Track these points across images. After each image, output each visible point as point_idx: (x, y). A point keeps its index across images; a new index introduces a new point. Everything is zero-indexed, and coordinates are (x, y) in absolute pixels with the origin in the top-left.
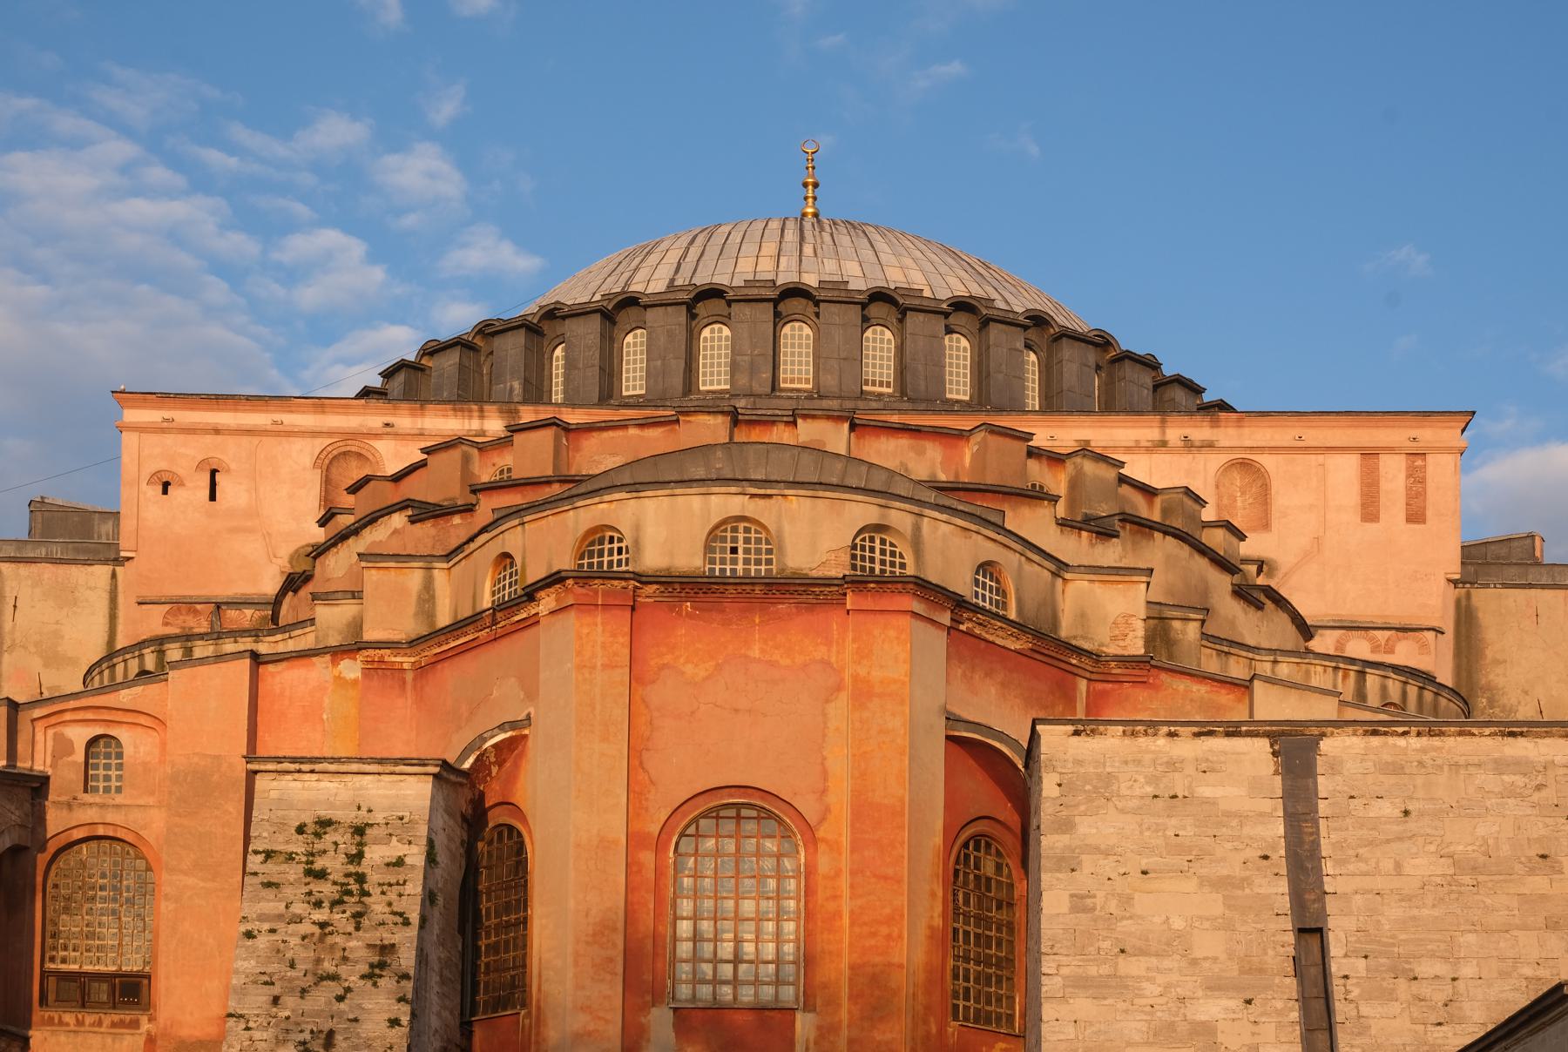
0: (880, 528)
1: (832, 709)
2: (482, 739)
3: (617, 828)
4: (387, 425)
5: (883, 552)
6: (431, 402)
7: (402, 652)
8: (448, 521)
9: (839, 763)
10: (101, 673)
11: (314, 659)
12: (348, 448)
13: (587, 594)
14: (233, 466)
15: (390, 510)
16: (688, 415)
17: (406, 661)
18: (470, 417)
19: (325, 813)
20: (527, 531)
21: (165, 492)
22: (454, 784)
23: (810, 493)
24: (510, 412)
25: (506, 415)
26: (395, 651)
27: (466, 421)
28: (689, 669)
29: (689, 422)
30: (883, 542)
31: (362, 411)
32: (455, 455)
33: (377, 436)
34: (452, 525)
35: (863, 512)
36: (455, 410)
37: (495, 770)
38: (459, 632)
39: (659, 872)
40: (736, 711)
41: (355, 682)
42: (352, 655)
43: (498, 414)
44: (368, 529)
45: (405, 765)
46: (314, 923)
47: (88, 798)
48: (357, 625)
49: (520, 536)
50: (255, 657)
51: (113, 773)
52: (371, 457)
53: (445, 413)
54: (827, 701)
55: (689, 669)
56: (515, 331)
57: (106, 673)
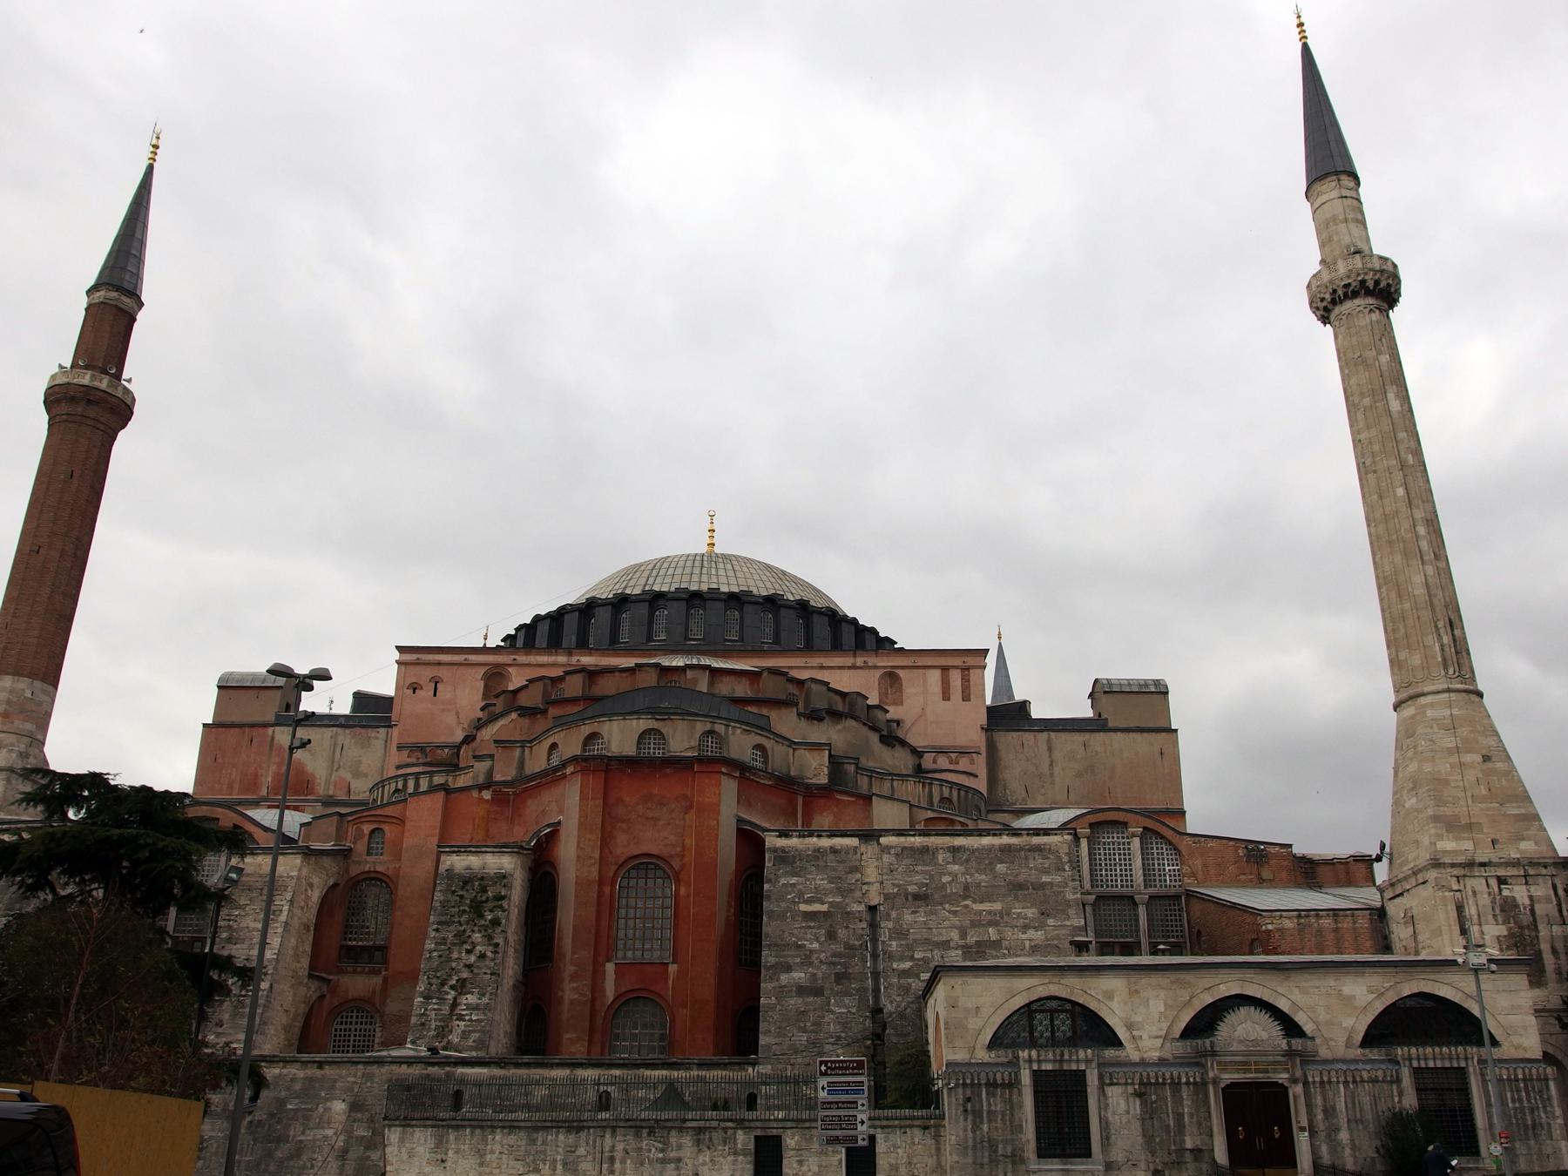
0: (711, 732)
1: (687, 816)
2: (540, 831)
3: (595, 874)
4: (515, 659)
5: (712, 742)
9: (690, 842)
10: (378, 789)
14: (445, 680)
18: (551, 655)
21: (414, 693)
22: (526, 854)
23: (681, 718)
28: (628, 799)
30: (712, 738)
32: (541, 684)
33: (510, 665)
35: (701, 727)
37: (544, 845)
39: (612, 896)
40: (647, 818)
41: (488, 801)
47: (368, 858)
48: (490, 773)
50: (446, 789)
51: (380, 846)
54: (686, 813)
55: (628, 799)
57: (380, 789)
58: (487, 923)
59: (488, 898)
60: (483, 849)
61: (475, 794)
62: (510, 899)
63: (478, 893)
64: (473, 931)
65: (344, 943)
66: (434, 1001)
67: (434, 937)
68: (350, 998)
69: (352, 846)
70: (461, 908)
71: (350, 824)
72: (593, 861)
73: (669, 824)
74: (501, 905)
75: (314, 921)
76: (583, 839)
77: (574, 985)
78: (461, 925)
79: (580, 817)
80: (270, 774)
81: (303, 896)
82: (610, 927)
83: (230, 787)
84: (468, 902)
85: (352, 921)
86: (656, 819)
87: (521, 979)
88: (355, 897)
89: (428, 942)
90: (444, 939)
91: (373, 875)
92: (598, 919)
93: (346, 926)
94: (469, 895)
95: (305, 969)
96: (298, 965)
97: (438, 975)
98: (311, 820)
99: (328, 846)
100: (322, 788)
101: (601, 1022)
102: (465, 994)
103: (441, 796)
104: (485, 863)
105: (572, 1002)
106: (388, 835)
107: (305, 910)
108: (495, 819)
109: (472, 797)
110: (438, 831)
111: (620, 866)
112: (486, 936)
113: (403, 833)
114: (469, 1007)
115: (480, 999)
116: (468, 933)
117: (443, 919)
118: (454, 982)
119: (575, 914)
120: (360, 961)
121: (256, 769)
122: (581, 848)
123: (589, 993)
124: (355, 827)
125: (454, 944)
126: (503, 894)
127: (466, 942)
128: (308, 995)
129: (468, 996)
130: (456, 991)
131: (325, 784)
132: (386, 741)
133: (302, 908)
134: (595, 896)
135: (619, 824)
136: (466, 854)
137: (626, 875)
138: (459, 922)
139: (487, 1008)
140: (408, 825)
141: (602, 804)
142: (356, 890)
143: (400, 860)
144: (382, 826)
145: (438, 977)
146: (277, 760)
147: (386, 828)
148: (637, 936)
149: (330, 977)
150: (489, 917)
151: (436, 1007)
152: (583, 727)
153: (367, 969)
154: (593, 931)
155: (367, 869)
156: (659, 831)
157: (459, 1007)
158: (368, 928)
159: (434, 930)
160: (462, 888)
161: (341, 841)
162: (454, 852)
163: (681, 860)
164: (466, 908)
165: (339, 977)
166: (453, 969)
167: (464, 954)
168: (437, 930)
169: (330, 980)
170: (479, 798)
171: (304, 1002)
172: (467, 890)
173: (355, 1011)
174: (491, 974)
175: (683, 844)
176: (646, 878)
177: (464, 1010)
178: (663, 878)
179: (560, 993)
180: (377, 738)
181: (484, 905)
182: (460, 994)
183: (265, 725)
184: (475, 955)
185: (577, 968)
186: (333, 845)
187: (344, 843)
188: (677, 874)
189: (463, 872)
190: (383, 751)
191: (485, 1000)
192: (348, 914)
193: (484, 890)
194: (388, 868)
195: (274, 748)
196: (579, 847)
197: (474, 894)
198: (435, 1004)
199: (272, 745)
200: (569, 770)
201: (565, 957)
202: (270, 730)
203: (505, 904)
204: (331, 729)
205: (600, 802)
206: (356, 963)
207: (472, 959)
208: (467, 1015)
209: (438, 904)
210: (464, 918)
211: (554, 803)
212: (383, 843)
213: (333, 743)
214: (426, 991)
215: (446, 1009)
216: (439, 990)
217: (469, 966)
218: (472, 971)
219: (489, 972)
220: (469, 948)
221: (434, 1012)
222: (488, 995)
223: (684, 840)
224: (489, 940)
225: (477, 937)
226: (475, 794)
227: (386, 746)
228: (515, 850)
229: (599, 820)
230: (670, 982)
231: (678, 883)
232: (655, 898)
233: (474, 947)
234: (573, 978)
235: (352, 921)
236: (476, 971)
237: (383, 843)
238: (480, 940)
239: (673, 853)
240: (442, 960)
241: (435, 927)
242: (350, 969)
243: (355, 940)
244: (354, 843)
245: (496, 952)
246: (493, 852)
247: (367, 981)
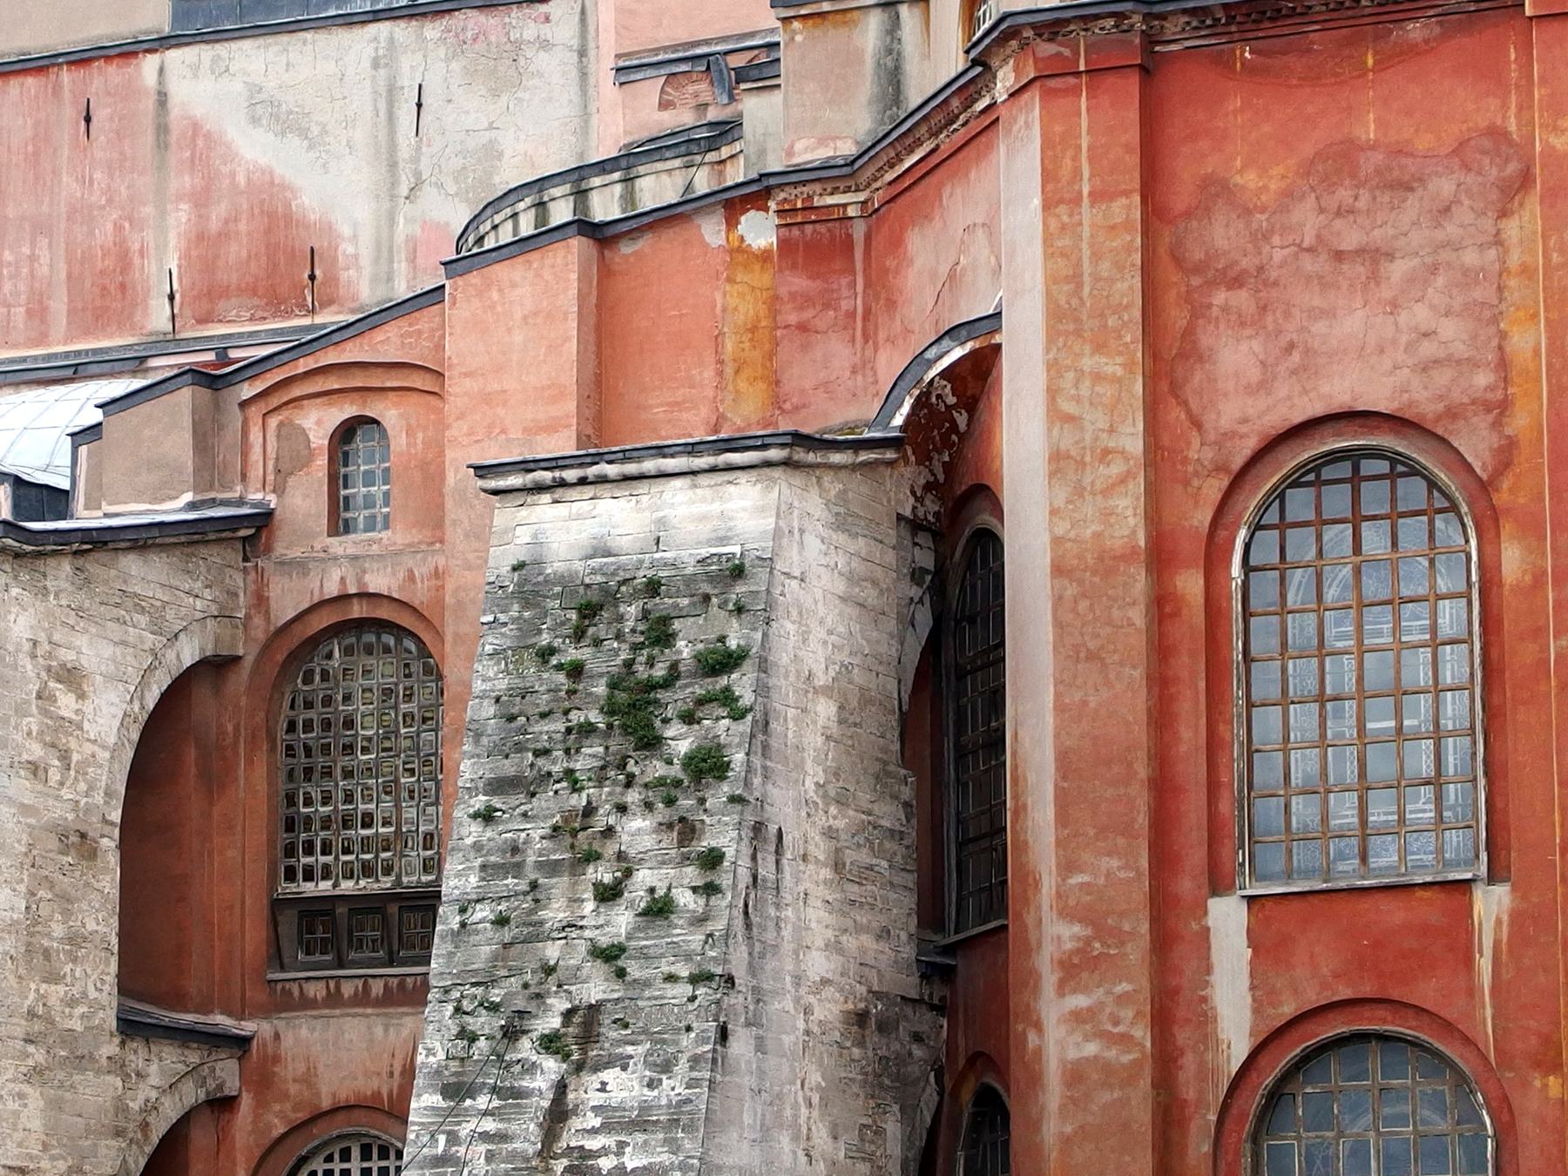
1: (1511, 229)
9: (1528, 341)
22: (854, 467)
37: (962, 419)
40: (1339, 256)
41: (764, 256)
47: (339, 545)
54: (1503, 214)
58: (676, 771)
59: (674, 666)
60: (649, 466)
61: (712, 230)
62: (764, 666)
63: (636, 648)
64: (622, 809)
65: (287, 889)
66: (482, 1101)
67: (477, 847)
68: (326, 1104)
69: (273, 501)
70: (576, 717)
71: (255, 412)
72: (1116, 468)
73: (1434, 269)
74: (727, 689)
75: (116, 816)
76: (1070, 375)
77: (1079, 1001)
78: (576, 787)
79: (1052, 280)
80: (173, 241)
81: (33, 723)
82: (1214, 745)
83: (38, 312)
84: (601, 689)
85: (308, 802)
86: (1375, 256)
87: (910, 985)
88: (309, 705)
89: (451, 866)
90: (515, 849)
91: (357, 611)
92: (1161, 719)
93: (290, 826)
94: (603, 662)
95: (96, 1006)
96: (56, 992)
97: (496, 995)
98: (97, 416)
99: (174, 509)
100: (367, 272)
101: (1206, 1148)
102: (596, 1069)
103: (572, 253)
104: (662, 523)
105: (1075, 1075)
106: (399, 441)
107: (54, 776)
108: (803, 328)
109: (706, 245)
110: (571, 406)
111: (1239, 480)
112: (670, 826)
113: (442, 425)
114: (618, 1122)
115: (651, 1085)
116: (601, 821)
117: (508, 767)
118: (555, 1022)
119: (1060, 708)
120: (353, 955)
121: (118, 228)
122: (1070, 419)
123: (1143, 1034)
124: (273, 422)
125: (552, 868)
126: (733, 643)
127: (592, 857)
128: (134, 1106)
129: (609, 1075)
130: (566, 1057)
131: (376, 261)
132: (582, 53)
133: (35, 769)
134: (1138, 616)
135: (1220, 297)
136: (589, 491)
137: (1272, 517)
138: (569, 773)
139: (677, 1119)
140: (458, 388)
141: (1137, 214)
142: (308, 679)
143: (442, 542)
144: (375, 408)
145: (494, 1008)
146: (186, 182)
147: (389, 413)
148: (1451, 762)
149: (248, 1027)
150: (683, 747)
151: (490, 1125)
153: (377, 988)
154: (1142, 771)
155: (332, 589)
156: (1394, 306)
157: (576, 1123)
158: (367, 824)
159: (475, 816)
160: (579, 635)
161: (225, 487)
162: (539, 488)
163: (1497, 424)
164: (595, 717)
165: (280, 1025)
166: (549, 970)
167: (589, 906)
168: (487, 817)
169: (242, 1043)
170: (731, 252)
171: (119, 1133)
172: (597, 643)
173: (356, 1153)
174: (694, 980)
175: (1500, 348)
176: (1357, 520)
177: (594, 1131)
178: (1431, 512)
179: (1032, 1039)
180: (544, 45)
181: (661, 695)
182: (579, 1068)
183: (127, 52)
184: (631, 905)
185: (1089, 932)
186: (192, 506)
187: (234, 494)
188: (1484, 488)
189: (578, 566)
190: (573, 91)
191: (673, 1087)
192: (291, 775)
193: (660, 634)
194: (411, 577)
195: (173, 138)
196: (1056, 416)
197: (623, 656)
198: (486, 1113)
199: (162, 129)
200: (1005, 79)
201: (1037, 884)
202: (150, 63)
203: (742, 684)
204: (373, 29)
205: (1128, 208)
206: (341, 966)
207: (621, 921)
208: (604, 1151)
209: (489, 709)
210: (589, 757)
211: (980, 232)
212: (387, 477)
213: (383, 90)
214: (454, 1066)
215: (527, 1134)
216: (500, 1057)
217: (609, 955)
218: (621, 973)
219: (684, 971)
220: (607, 878)
221: (483, 1148)
222: (682, 1067)
223: (1503, 335)
224: (681, 843)
225: (638, 832)
226: (712, 230)
227: (584, 75)
228: (774, 454)
229: (1129, 287)
230: (1484, 964)
231: (1489, 524)
232: (1395, 602)
233: (628, 873)
234: (1074, 970)
235: (308, 802)
236: (634, 970)
237: (387, 477)
238: (648, 842)
239: (1457, 396)
240: (507, 934)
241: (480, 802)
242: (316, 990)
243: (326, 874)
244: (279, 490)
245: (710, 889)
246: (694, 473)
247: (379, 1031)
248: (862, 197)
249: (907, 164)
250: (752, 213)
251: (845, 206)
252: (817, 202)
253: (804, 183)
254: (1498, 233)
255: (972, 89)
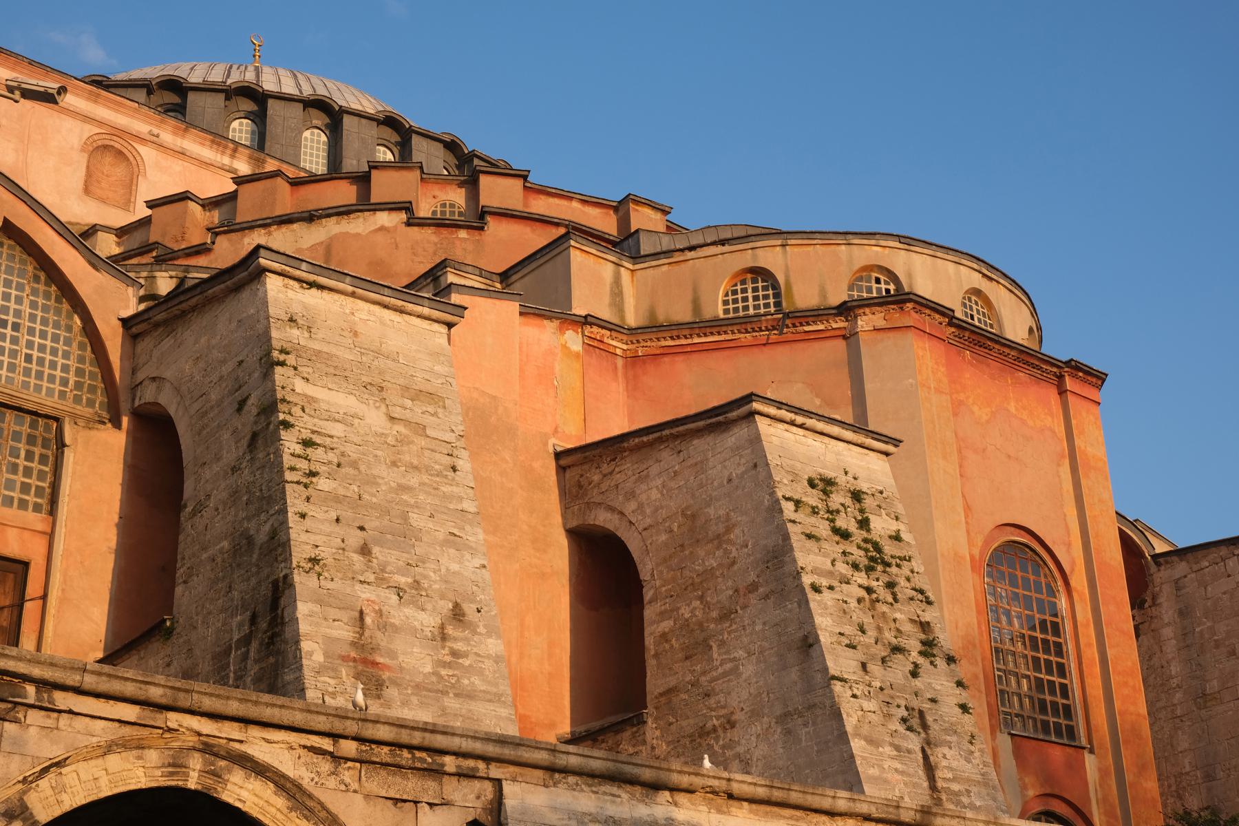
6: (195, 127)
7: (621, 336)
8: (452, 233)
11: (546, 322)
12: (112, 143)
13: (919, 320)
15: (378, 207)
16: (637, 205)
17: (619, 346)
18: (223, 153)
19: (830, 474)
20: (789, 253)
24: (258, 160)
25: (253, 161)
26: (614, 334)
27: (219, 155)
28: (975, 409)
29: (637, 210)
31: (131, 113)
33: (143, 140)
34: (457, 237)
36: (213, 142)
38: (714, 330)
41: (577, 355)
42: (575, 328)
43: (246, 158)
44: (334, 219)
45: (873, 438)
46: (860, 586)
49: (780, 255)
52: (131, 159)
53: (203, 141)
54: (1059, 465)
56: (213, 94)
136: (801, 431)
152: (843, 247)
175: (1065, 520)
248: (625, 347)
249: (696, 340)
250: (571, 332)
251: (616, 347)
252: (606, 340)
253: (603, 327)
254: (1058, 472)
255: (810, 319)
